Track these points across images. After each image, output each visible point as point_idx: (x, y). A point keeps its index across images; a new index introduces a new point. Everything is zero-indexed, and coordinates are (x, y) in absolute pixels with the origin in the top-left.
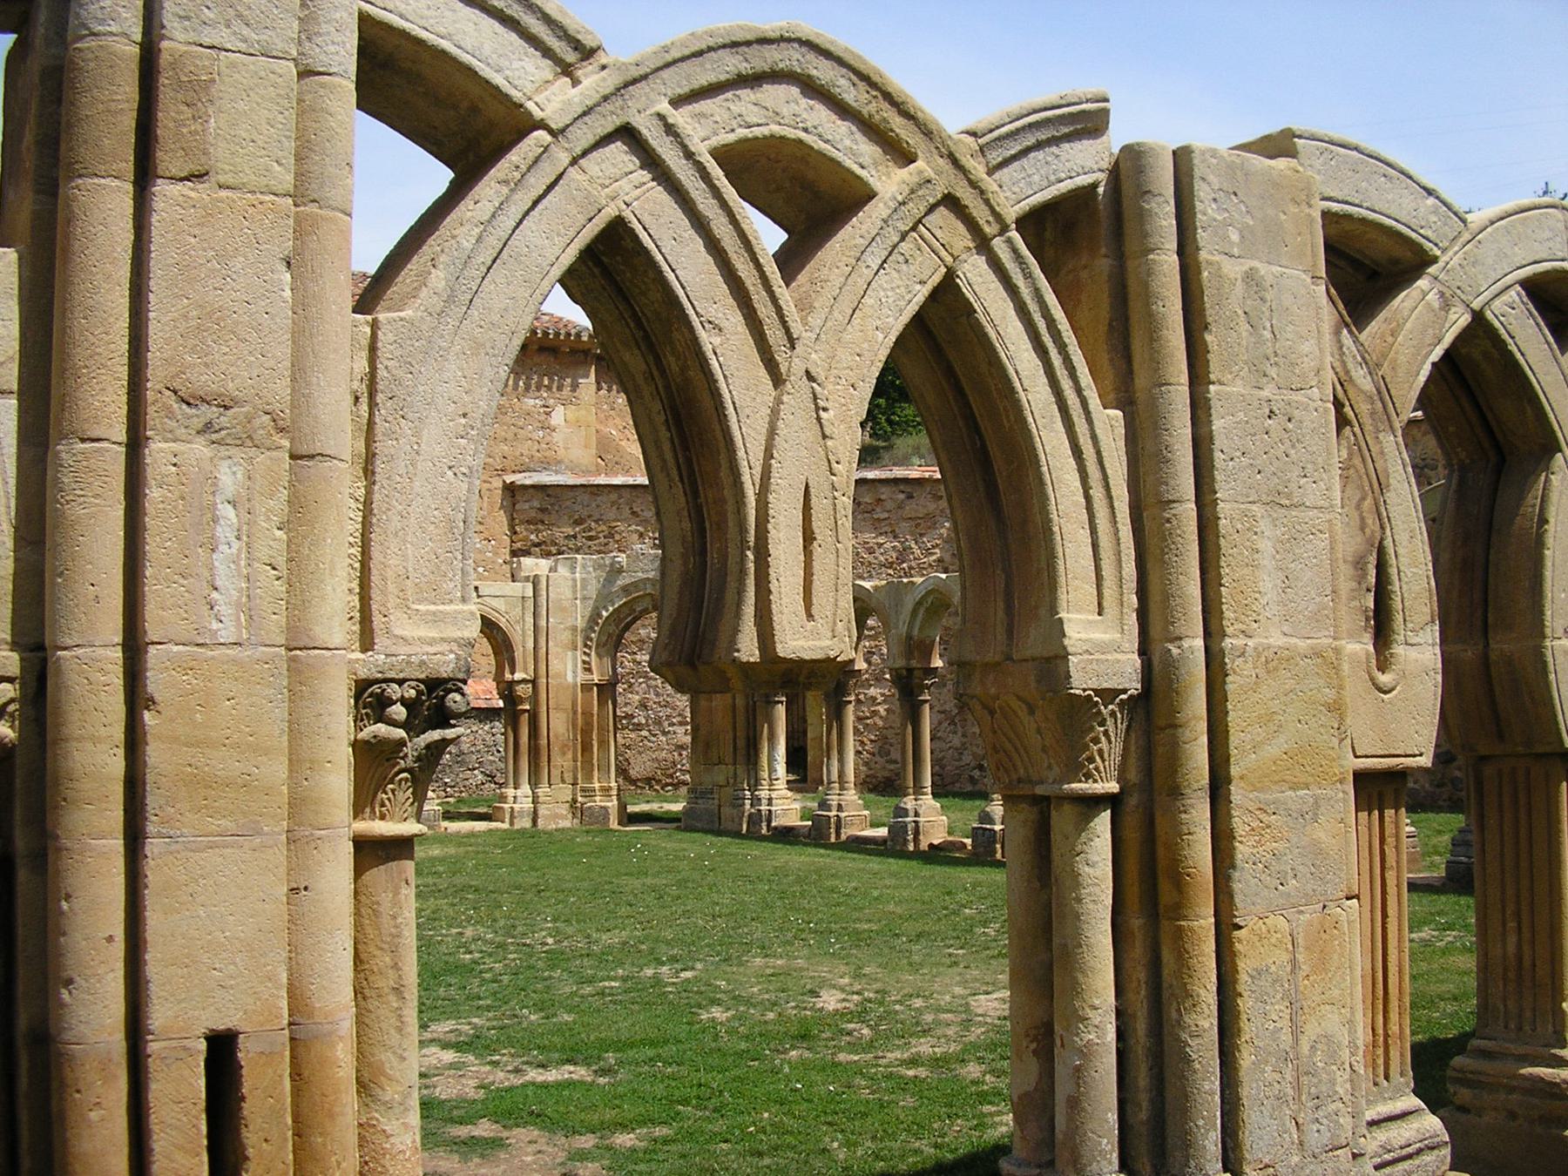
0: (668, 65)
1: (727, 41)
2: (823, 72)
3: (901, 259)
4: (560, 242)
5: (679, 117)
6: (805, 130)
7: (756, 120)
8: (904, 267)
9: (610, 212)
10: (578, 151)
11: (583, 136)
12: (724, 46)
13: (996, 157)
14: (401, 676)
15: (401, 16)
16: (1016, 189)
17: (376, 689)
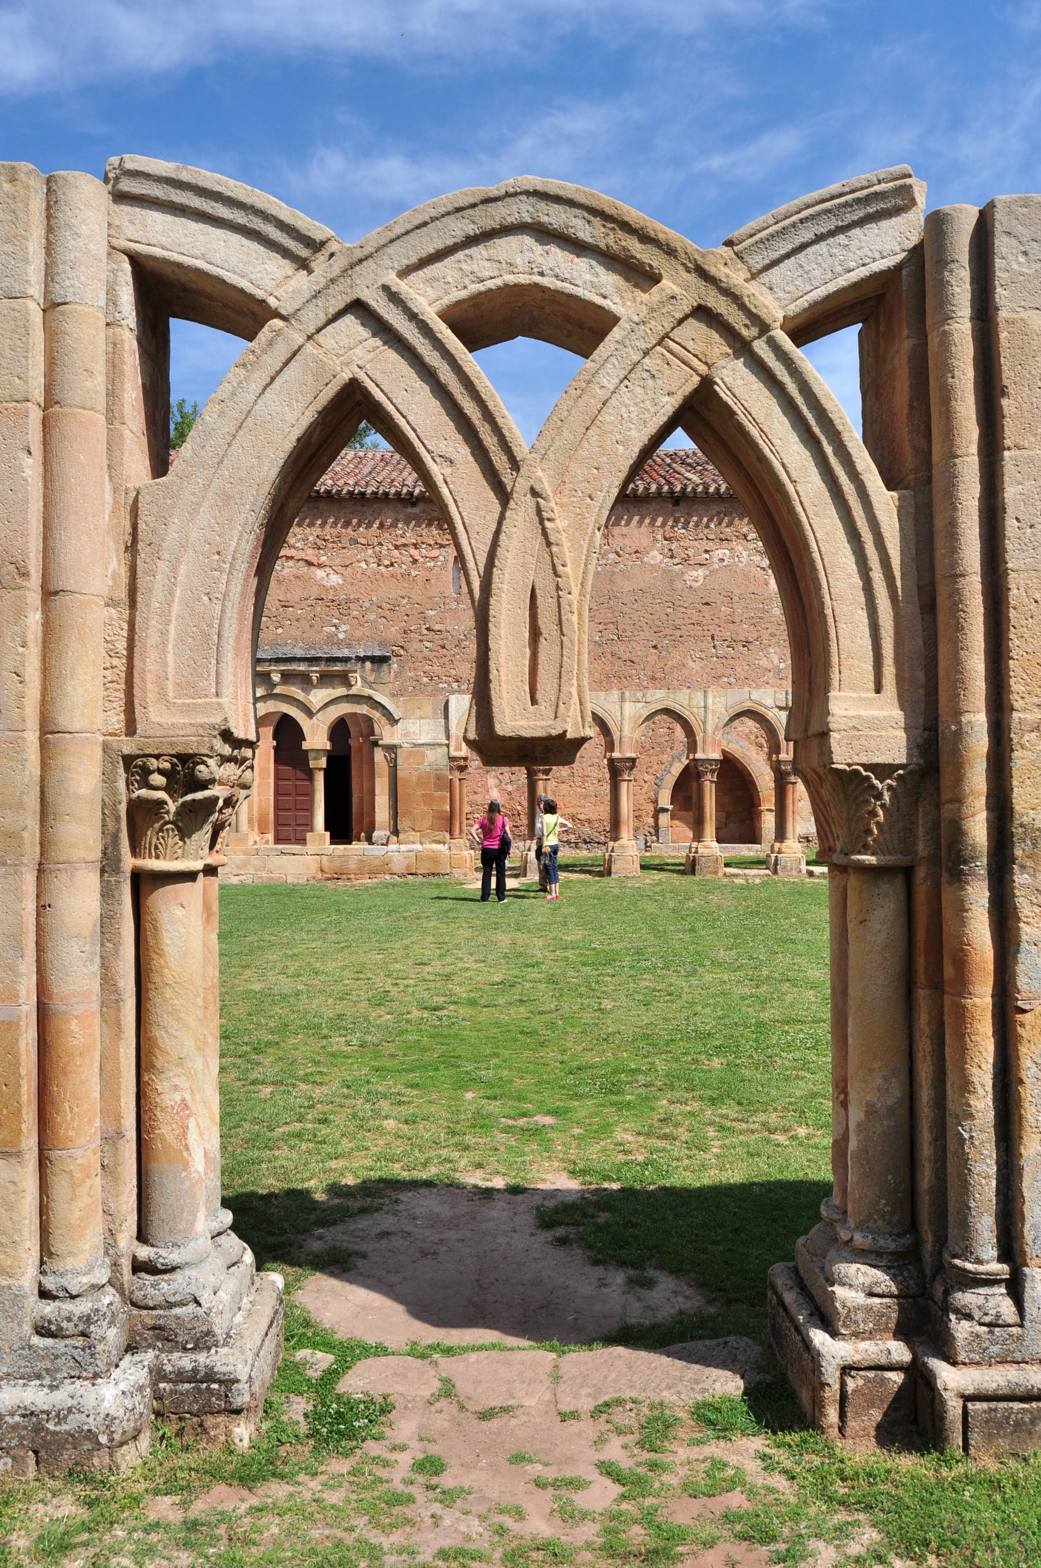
0: (392, 241)
1: (450, 208)
2: (555, 216)
3: (646, 375)
4: (298, 407)
5: (402, 286)
6: (542, 274)
7: (487, 274)
8: (650, 382)
9: (346, 376)
10: (312, 329)
11: (314, 316)
12: (448, 214)
13: (757, 261)
14: (156, 752)
15: (163, 247)
16: (791, 288)
17: (139, 762)
